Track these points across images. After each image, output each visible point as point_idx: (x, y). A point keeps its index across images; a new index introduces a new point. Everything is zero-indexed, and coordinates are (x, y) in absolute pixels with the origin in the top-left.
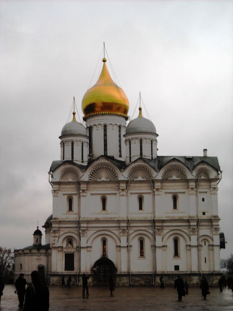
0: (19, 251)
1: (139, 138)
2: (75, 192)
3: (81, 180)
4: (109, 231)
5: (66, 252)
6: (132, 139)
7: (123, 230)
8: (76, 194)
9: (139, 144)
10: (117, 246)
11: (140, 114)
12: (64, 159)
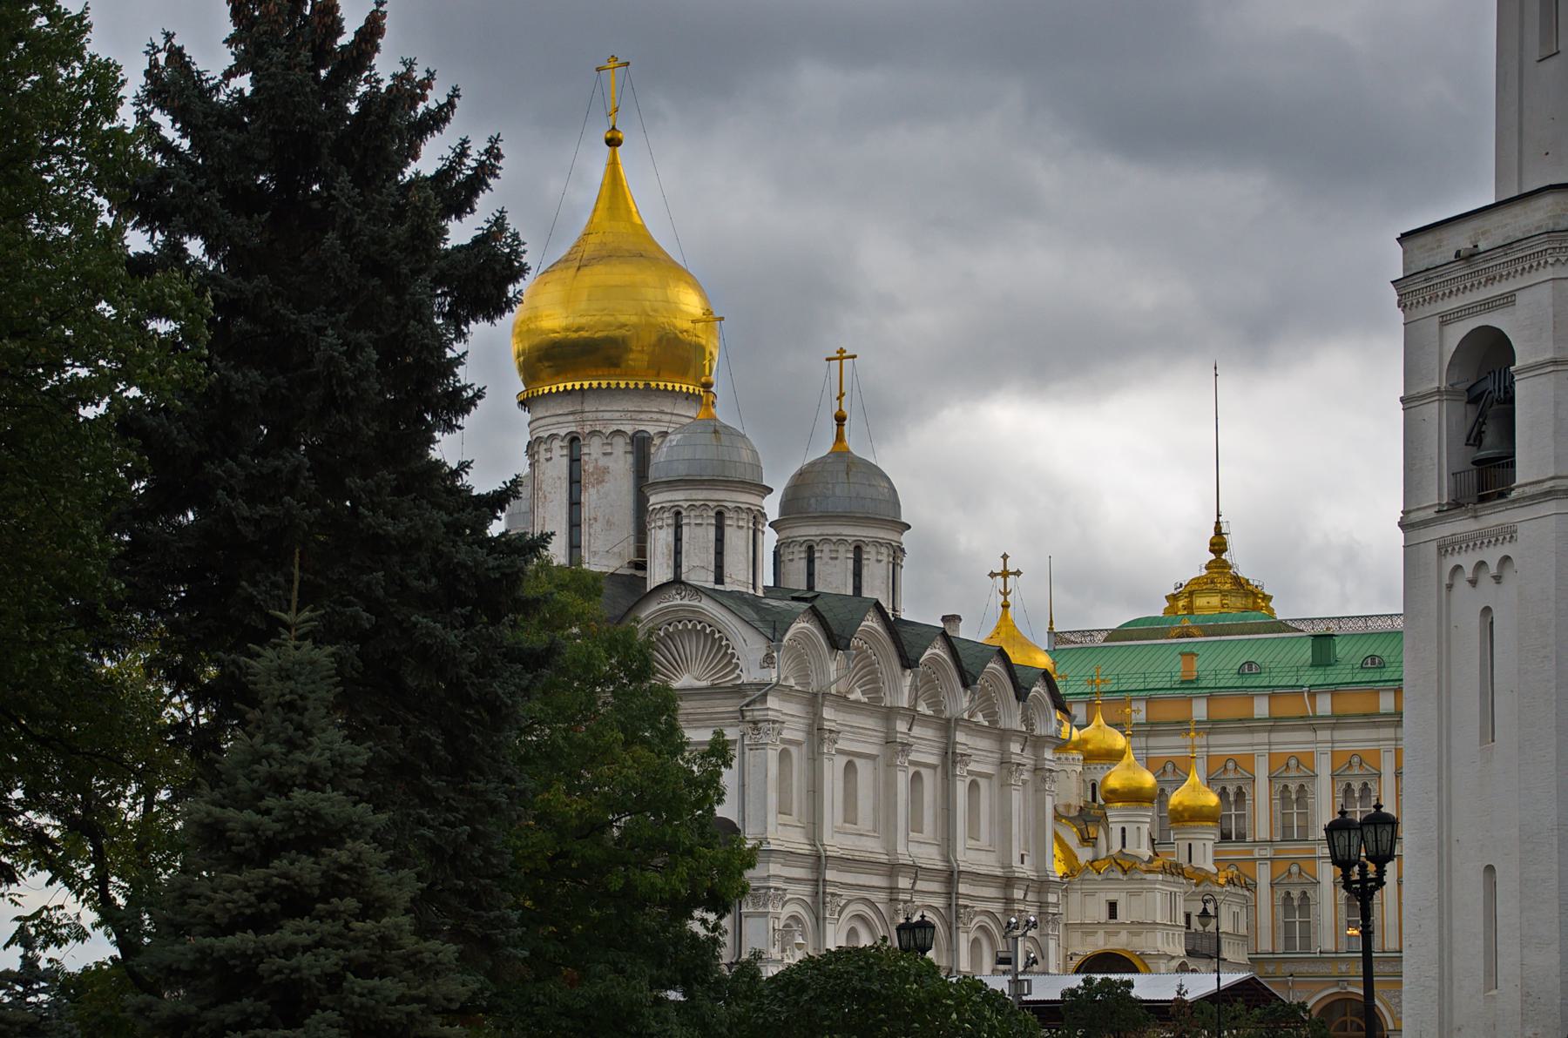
11: (840, 437)
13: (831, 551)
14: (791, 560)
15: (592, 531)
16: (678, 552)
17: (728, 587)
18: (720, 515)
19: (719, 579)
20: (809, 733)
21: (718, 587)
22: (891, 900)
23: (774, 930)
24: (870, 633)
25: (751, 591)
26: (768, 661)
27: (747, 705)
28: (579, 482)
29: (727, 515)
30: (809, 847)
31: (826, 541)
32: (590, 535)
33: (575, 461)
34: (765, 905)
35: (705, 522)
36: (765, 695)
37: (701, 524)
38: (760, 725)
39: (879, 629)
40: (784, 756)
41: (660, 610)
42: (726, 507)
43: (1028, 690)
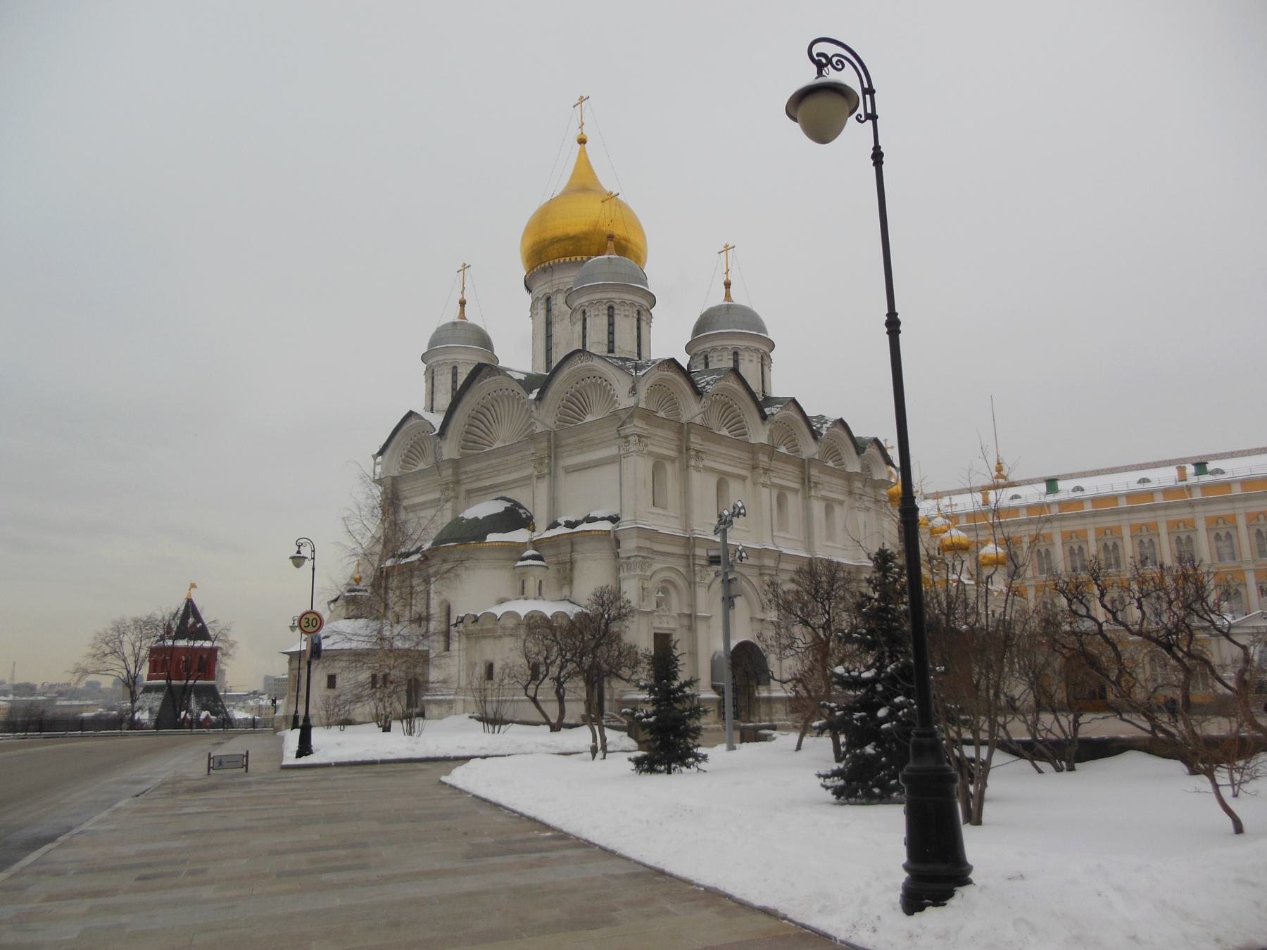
2: (672, 454)
5: (658, 628)
6: (714, 349)
7: (771, 575)
9: (760, 365)
10: (751, 619)
11: (728, 296)
15: (558, 350)
16: (584, 337)
18: (611, 308)
19: (611, 350)
20: (681, 452)
21: (610, 355)
23: (643, 589)
26: (633, 391)
28: (551, 323)
29: (615, 307)
32: (556, 353)
33: (549, 310)
37: (598, 315)
38: (630, 438)
42: (614, 302)
43: (864, 449)
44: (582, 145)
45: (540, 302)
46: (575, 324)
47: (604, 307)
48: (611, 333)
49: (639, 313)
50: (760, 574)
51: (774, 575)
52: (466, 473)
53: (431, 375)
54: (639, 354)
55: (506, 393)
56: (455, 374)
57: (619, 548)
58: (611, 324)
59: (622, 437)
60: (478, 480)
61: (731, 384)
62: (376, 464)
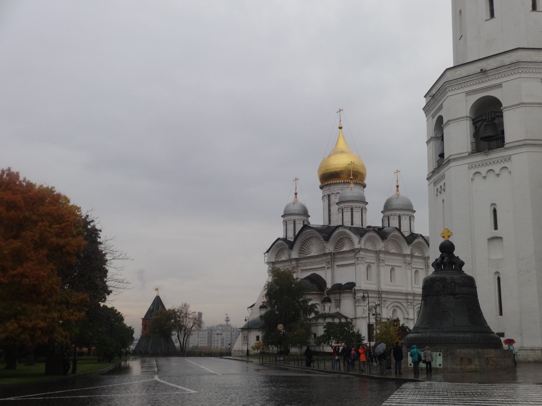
0: (312, 320)
1: (410, 215)
3: (381, 250)
4: (400, 303)
7: (411, 302)
8: (374, 263)
9: (409, 220)
10: (404, 318)
11: (398, 191)
12: (352, 224)
13: (393, 217)
14: (385, 221)
16: (343, 219)
17: (354, 226)
18: (352, 209)
19: (352, 224)
20: (377, 260)
22: (407, 302)
23: (363, 310)
24: (396, 236)
25: (361, 227)
27: (356, 254)
28: (330, 205)
29: (354, 209)
30: (377, 289)
31: (392, 215)
33: (329, 200)
34: (361, 303)
35: (348, 211)
36: (359, 251)
39: (399, 235)
40: (368, 267)
41: (338, 232)
44: (341, 129)
45: (326, 197)
46: (339, 213)
47: (349, 208)
48: (352, 218)
49: (362, 209)
50: (407, 302)
51: (412, 302)
52: (301, 263)
53: (286, 223)
54: (362, 225)
55: (315, 236)
56: (295, 224)
57: (355, 295)
58: (352, 215)
59: (356, 258)
60: (305, 266)
61: (395, 233)
62: (265, 256)
